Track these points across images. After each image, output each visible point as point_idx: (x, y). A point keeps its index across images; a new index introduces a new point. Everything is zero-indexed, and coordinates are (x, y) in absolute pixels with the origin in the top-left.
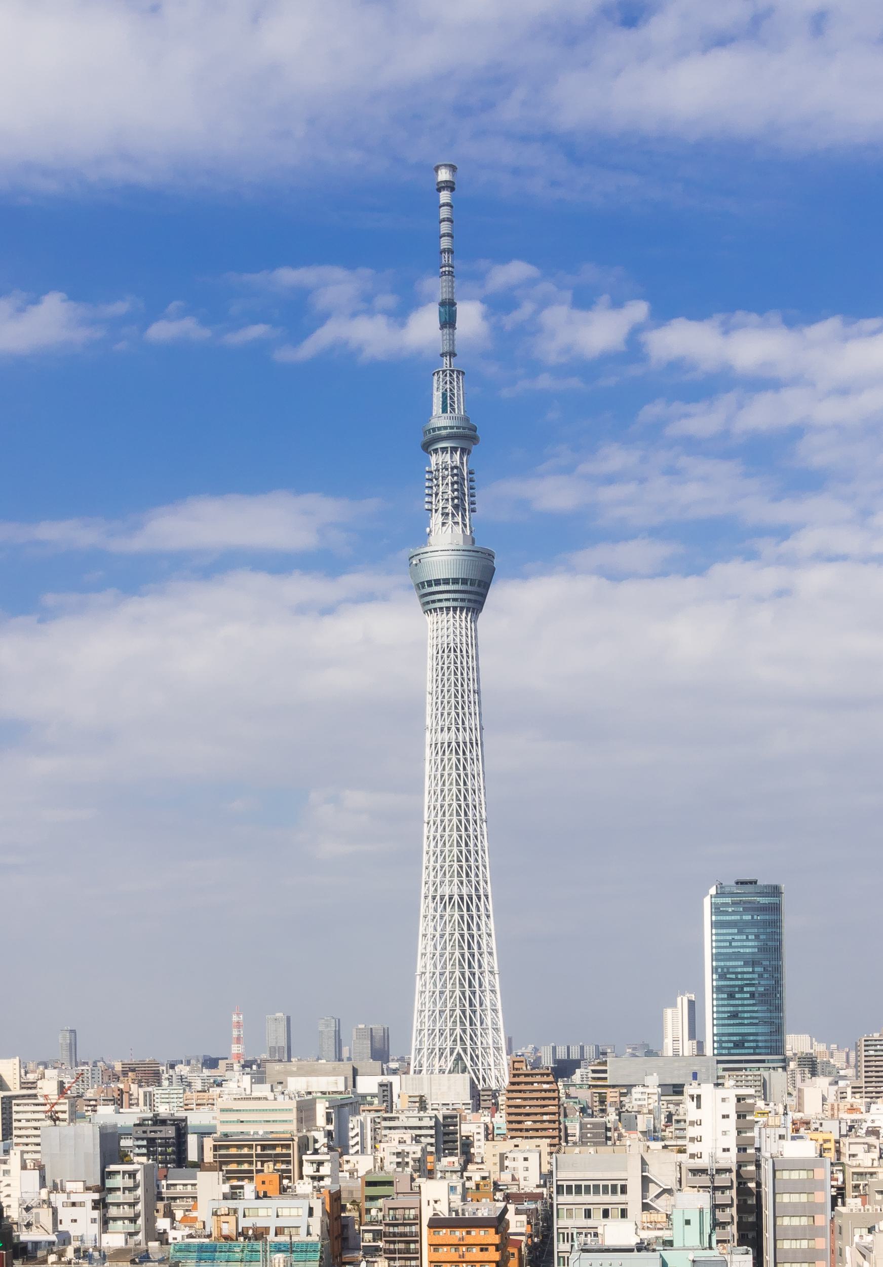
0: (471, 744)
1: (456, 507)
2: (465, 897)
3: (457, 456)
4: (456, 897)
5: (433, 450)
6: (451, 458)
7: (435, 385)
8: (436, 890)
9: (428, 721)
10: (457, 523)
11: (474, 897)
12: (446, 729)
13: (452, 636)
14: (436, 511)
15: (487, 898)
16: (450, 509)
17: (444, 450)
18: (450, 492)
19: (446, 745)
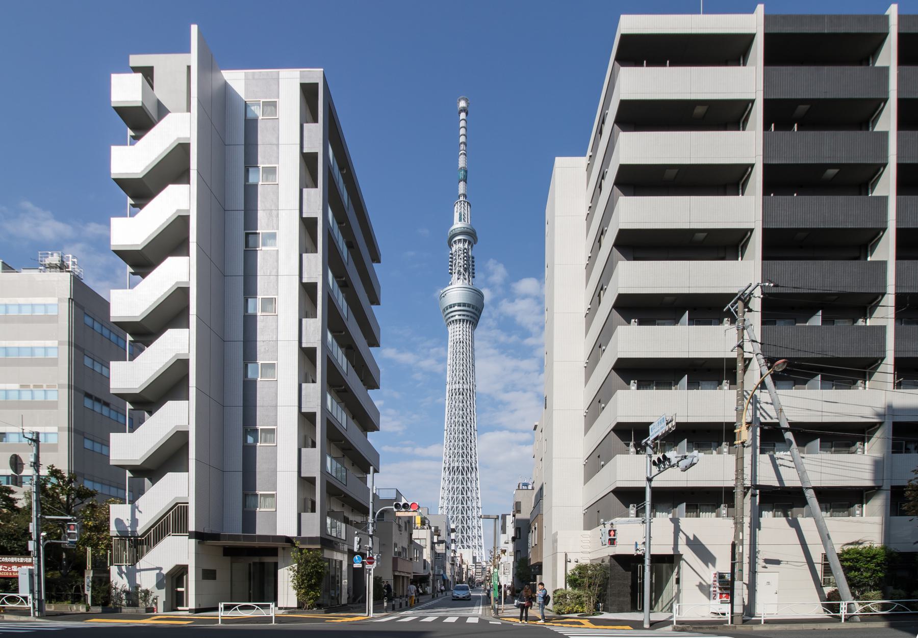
0: (470, 390)
1: (465, 270)
2: (465, 468)
3: (466, 246)
4: (461, 468)
5: (454, 242)
6: (464, 245)
7: (455, 210)
8: (450, 464)
9: (448, 379)
10: (465, 279)
11: (470, 468)
12: (457, 382)
13: (462, 335)
14: (455, 273)
15: (477, 470)
16: (462, 270)
17: (459, 240)
18: (462, 262)
19: (457, 390)
